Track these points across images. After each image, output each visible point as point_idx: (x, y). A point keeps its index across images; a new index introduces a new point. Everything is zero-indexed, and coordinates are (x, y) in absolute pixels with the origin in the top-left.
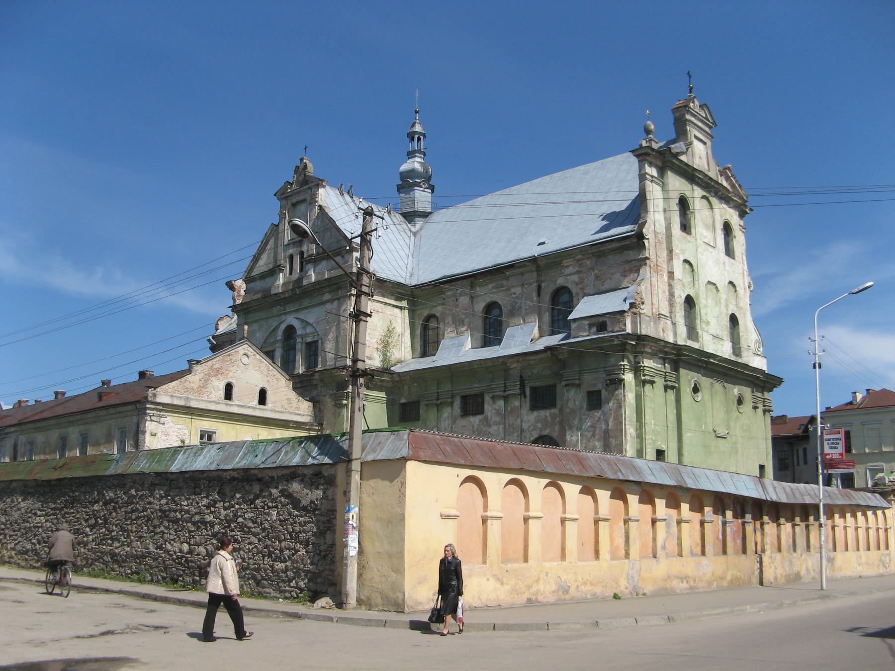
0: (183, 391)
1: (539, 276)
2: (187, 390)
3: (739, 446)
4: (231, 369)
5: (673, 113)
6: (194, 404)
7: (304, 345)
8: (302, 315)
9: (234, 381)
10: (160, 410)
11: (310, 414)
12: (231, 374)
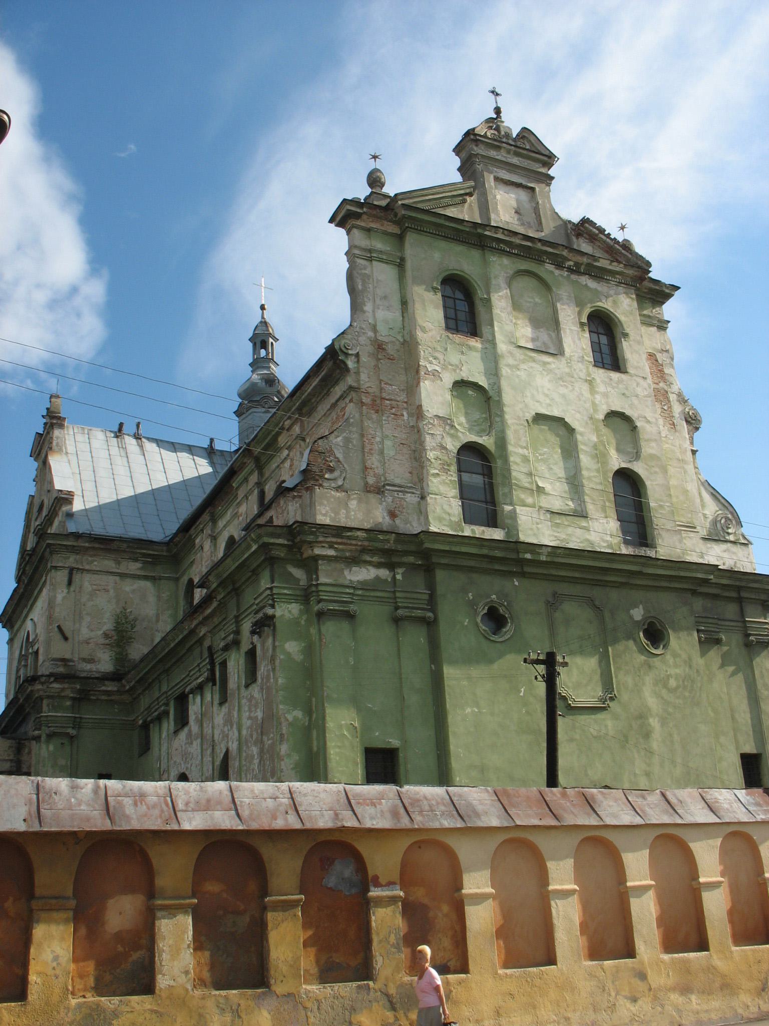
1: (261, 474)
3: (654, 722)
5: (457, 154)
11: (11, 757)
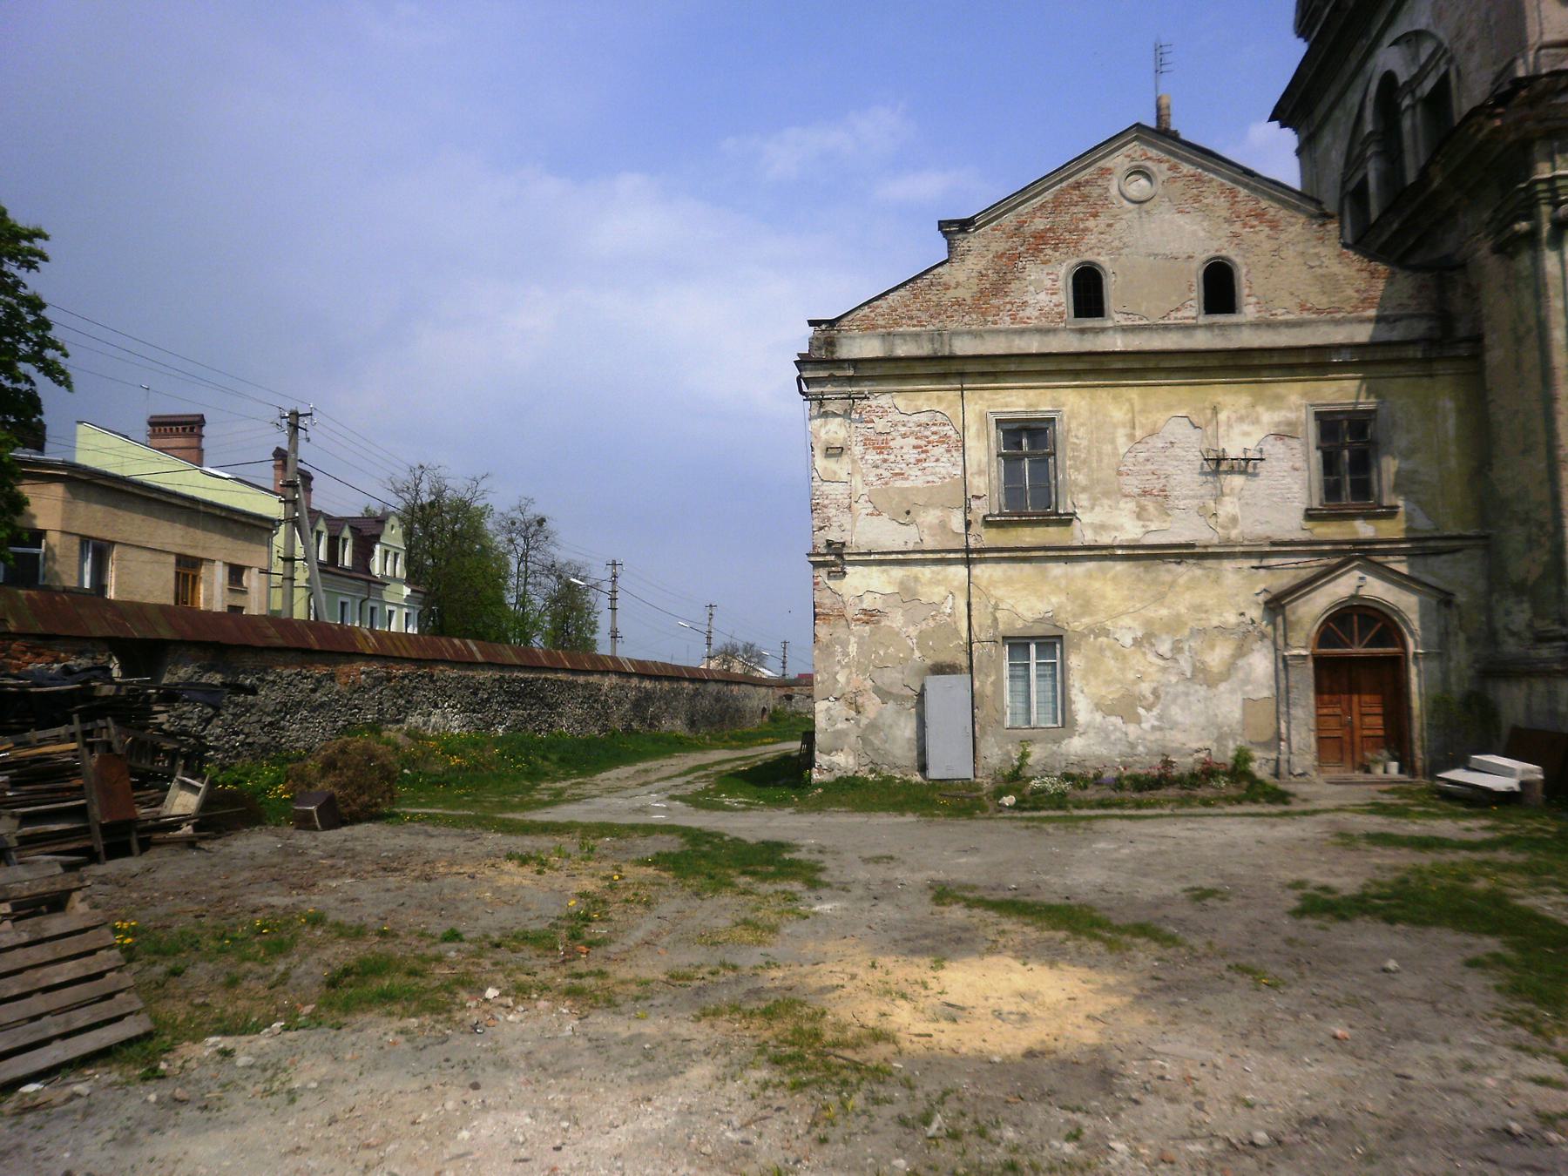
0: (924, 317)
2: (938, 311)
4: (1091, 223)
6: (964, 347)
7: (1419, 109)
8: (1402, 27)
9: (1103, 260)
10: (850, 380)
12: (1091, 239)
